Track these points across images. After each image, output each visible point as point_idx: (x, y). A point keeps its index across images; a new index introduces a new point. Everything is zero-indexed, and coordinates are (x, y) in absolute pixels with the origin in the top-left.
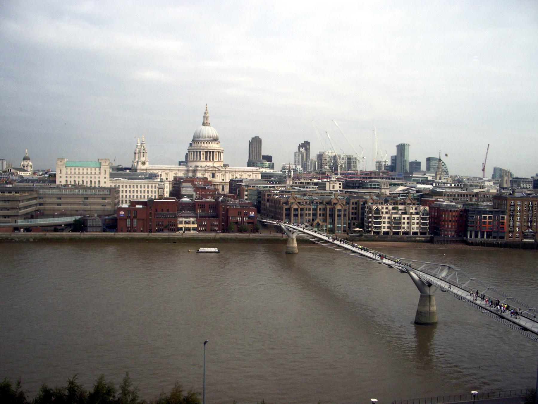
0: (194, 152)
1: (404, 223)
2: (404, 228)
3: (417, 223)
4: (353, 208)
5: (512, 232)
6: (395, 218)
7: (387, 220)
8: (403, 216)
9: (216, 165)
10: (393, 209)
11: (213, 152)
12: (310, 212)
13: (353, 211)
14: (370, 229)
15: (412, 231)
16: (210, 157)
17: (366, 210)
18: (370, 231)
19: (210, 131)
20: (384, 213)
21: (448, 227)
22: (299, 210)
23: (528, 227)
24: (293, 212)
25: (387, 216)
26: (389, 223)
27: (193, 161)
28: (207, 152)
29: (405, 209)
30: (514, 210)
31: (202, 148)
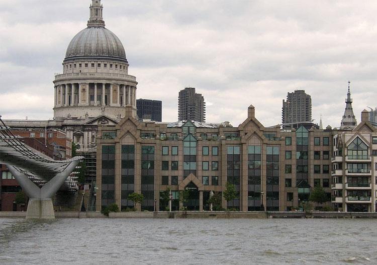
0: (64, 86)
4: (317, 153)
9: (111, 115)
11: (108, 86)
12: (176, 159)
13: (317, 162)
14: (338, 200)
16: (99, 98)
17: (335, 149)
18: (340, 205)
19: (104, 39)
22: (138, 148)
24: (119, 156)
27: (62, 107)
28: (92, 86)
31: (80, 76)
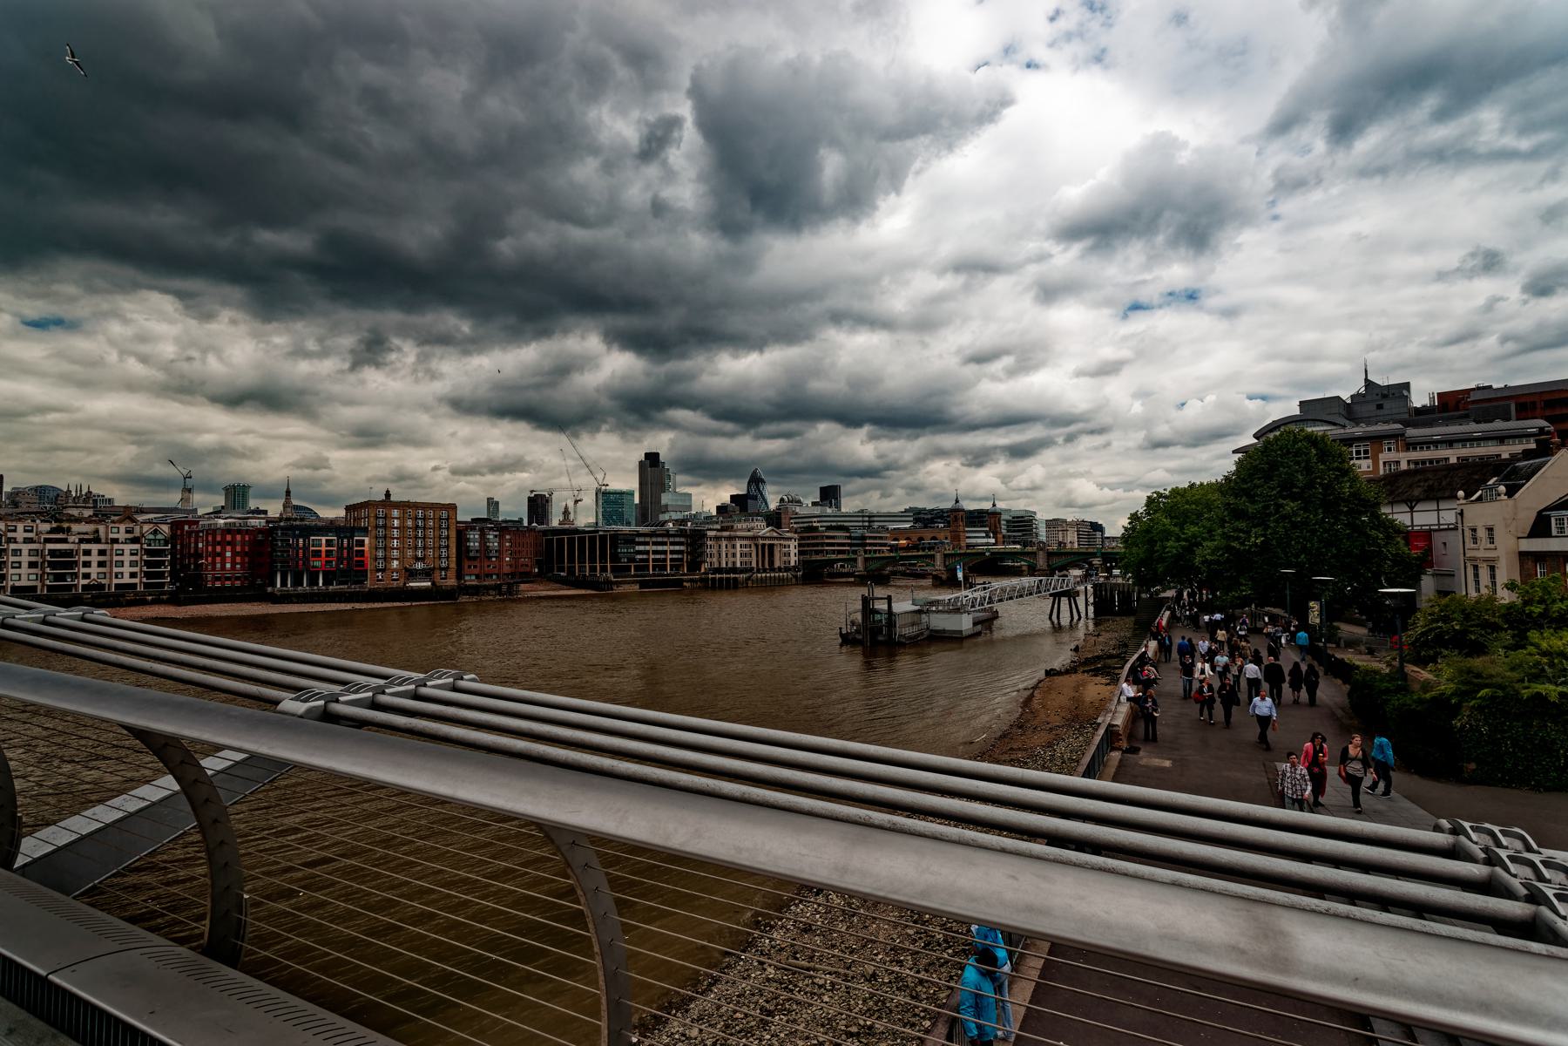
1: (87, 564)
2: (87, 576)
3: (133, 564)
5: (383, 571)
6: (53, 553)
7: (25, 559)
8: (84, 546)
10: (52, 531)
15: (115, 581)
20: (20, 539)
21: (223, 567)
23: (417, 559)
25: (25, 548)
26: (32, 565)
29: (97, 531)
30: (385, 526)
